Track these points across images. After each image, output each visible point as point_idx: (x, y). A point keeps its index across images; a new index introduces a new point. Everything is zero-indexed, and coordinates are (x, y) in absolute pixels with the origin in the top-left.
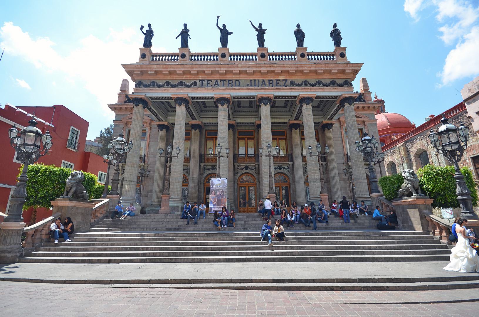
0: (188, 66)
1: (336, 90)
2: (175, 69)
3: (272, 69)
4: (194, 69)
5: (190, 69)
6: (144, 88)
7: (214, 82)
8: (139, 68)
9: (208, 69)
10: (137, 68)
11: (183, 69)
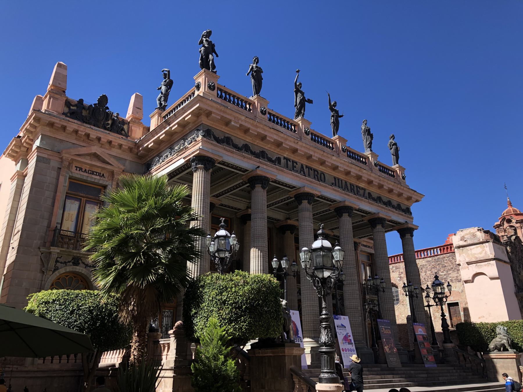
0: (282, 135)
1: (402, 216)
2: (266, 133)
3: (360, 174)
4: (287, 142)
5: (283, 141)
6: (215, 143)
7: (298, 167)
8: (221, 111)
9: (303, 149)
10: (217, 109)
11: (275, 137)
